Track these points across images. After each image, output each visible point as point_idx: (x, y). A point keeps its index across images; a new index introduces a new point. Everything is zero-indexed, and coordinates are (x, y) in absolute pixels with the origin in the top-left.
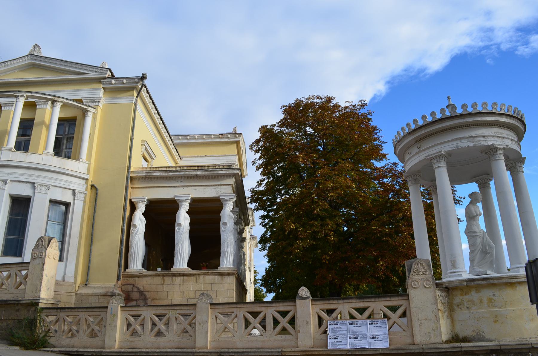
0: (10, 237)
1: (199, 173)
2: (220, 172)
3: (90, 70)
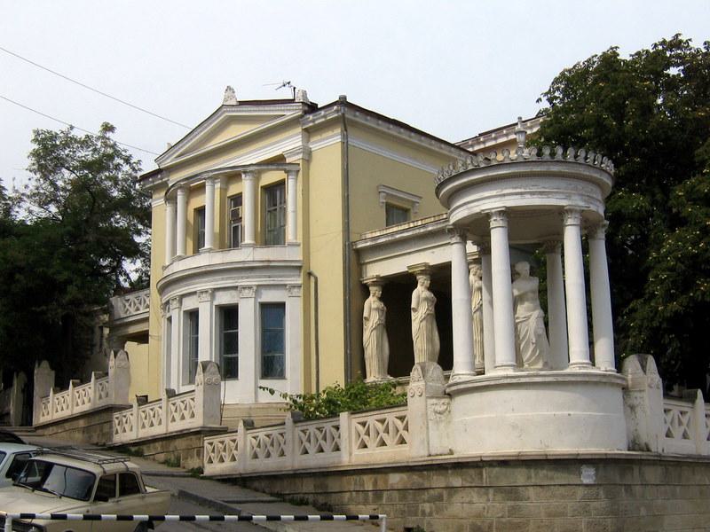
0: (234, 355)
1: (430, 228)
3: (284, 110)
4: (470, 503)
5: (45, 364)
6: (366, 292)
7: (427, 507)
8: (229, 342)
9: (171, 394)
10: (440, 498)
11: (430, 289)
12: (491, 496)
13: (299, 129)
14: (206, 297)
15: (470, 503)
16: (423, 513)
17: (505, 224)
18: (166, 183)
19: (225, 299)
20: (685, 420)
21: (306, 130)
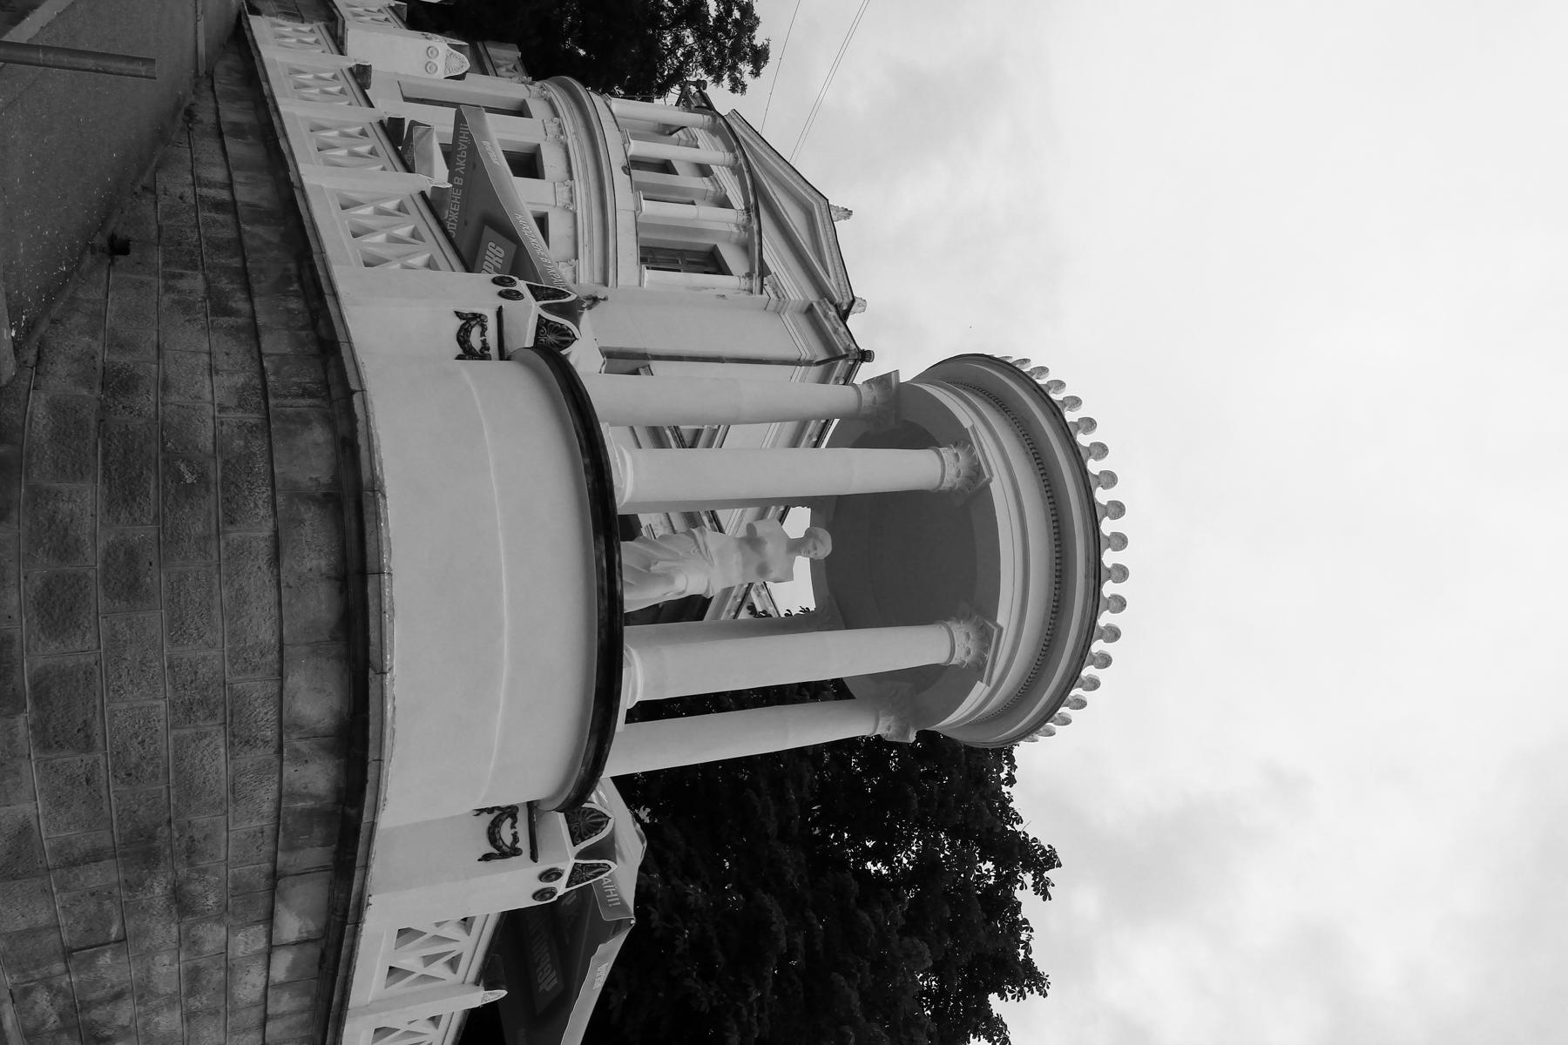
4: (212, 370)
7: (194, 283)
12: (234, 417)
13: (812, 297)
14: (552, 128)
15: (212, 370)
17: (946, 485)
19: (551, 160)
20: (439, 969)
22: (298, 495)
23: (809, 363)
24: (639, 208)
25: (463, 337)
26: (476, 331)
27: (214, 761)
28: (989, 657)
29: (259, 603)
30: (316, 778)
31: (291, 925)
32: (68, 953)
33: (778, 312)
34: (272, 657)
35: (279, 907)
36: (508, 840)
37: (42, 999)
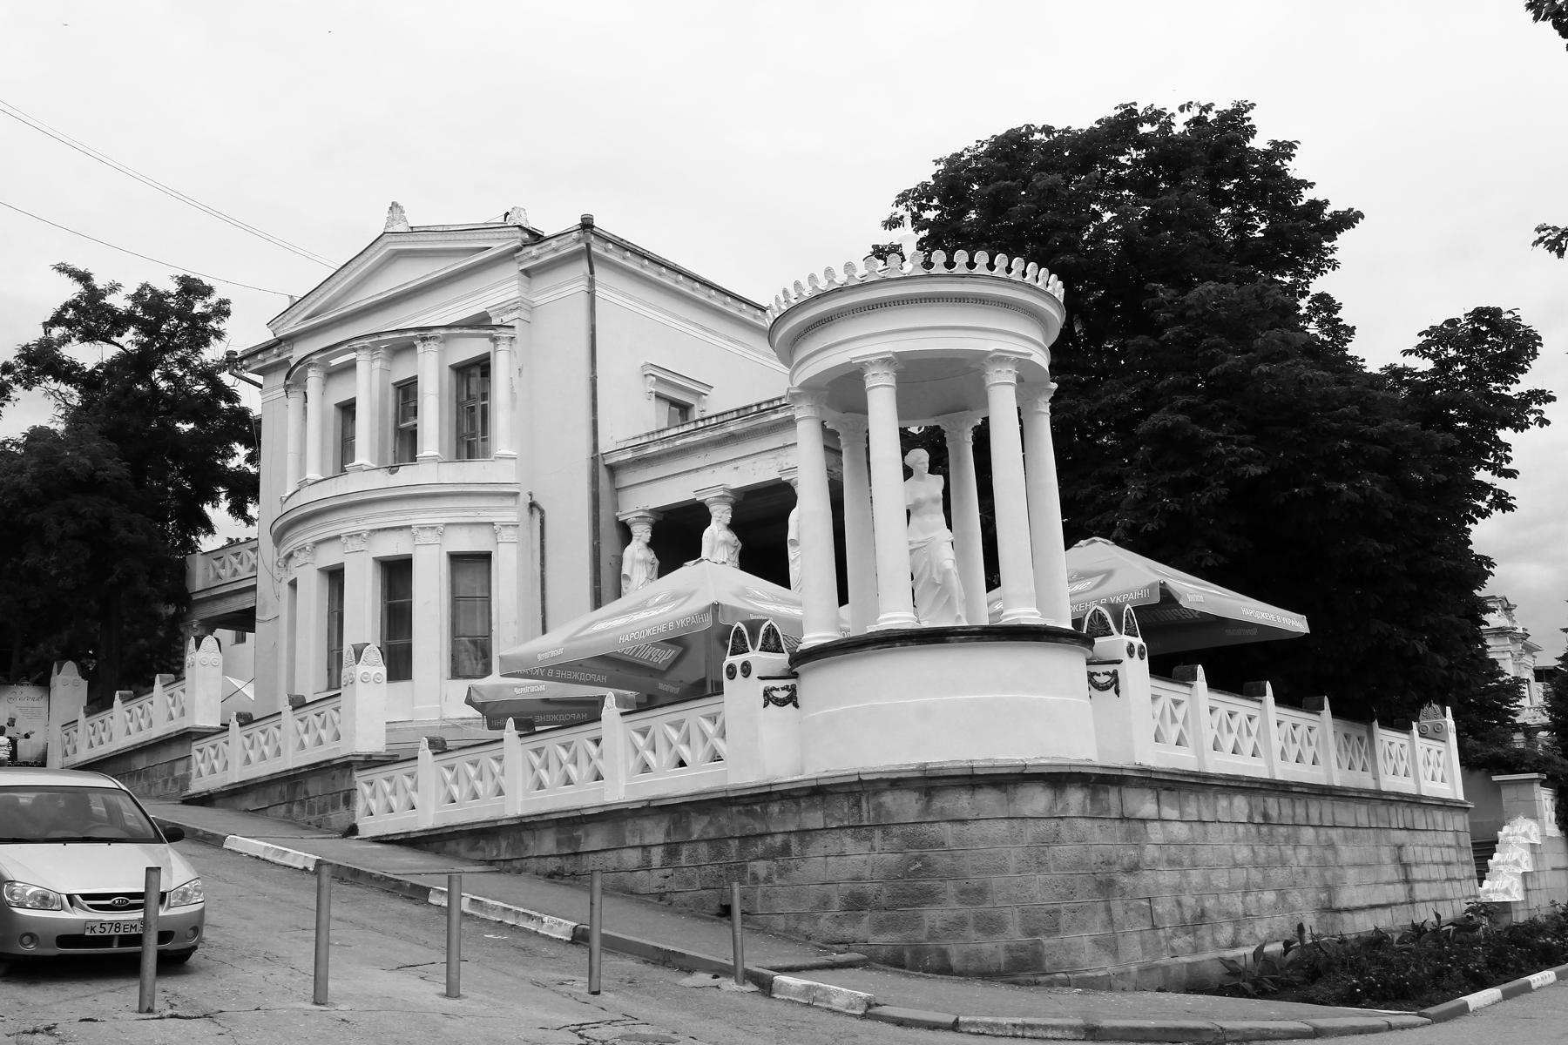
1: (732, 429)
2: (774, 417)
5: (70, 667)
6: (625, 533)
7: (761, 867)
8: (397, 617)
9: (298, 704)
10: (785, 850)
11: (732, 526)
12: (877, 842)
13: (512, 270)
14: (354, 544)
15: (841, 855)
16: (755, 877)
18: (286, 362)
19: (392, 547)
20: (1180, 713)
21: (526, 272)
22: (926, 809)
23: (592, 282)
24: (434, 459)
25: (781, 703)
26: (775, 694)
27: (1066, 852)
28: (1013, 356)
29: (985, 833)
30: (1075, 798)
31: (1148, 808)
32: (1154, 927)
33: (532, 309)
34: (1015, 822)
35: (1139, 815)
36: (1107, 678)
37: (1177, 942)
